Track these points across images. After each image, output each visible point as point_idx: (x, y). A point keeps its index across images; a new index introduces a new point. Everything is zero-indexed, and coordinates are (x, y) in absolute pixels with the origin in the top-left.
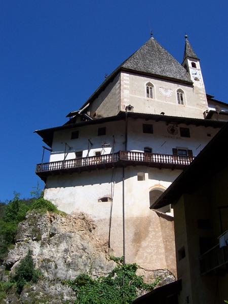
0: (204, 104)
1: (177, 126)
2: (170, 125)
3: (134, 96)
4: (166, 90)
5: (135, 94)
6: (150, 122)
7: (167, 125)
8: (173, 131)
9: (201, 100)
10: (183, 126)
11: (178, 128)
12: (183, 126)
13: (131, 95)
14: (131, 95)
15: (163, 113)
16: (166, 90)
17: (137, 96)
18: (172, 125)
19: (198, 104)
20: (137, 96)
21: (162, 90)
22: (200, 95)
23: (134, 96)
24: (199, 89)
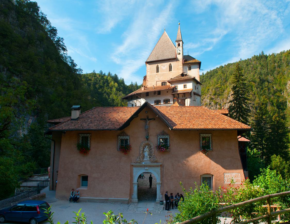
4: (164, 66)
5: (152, 73)
13: (150, 74)
14: (150, 74)
17: (152, 74)
19: (178, 69)
20: (152, 74)
21: (162, 67)
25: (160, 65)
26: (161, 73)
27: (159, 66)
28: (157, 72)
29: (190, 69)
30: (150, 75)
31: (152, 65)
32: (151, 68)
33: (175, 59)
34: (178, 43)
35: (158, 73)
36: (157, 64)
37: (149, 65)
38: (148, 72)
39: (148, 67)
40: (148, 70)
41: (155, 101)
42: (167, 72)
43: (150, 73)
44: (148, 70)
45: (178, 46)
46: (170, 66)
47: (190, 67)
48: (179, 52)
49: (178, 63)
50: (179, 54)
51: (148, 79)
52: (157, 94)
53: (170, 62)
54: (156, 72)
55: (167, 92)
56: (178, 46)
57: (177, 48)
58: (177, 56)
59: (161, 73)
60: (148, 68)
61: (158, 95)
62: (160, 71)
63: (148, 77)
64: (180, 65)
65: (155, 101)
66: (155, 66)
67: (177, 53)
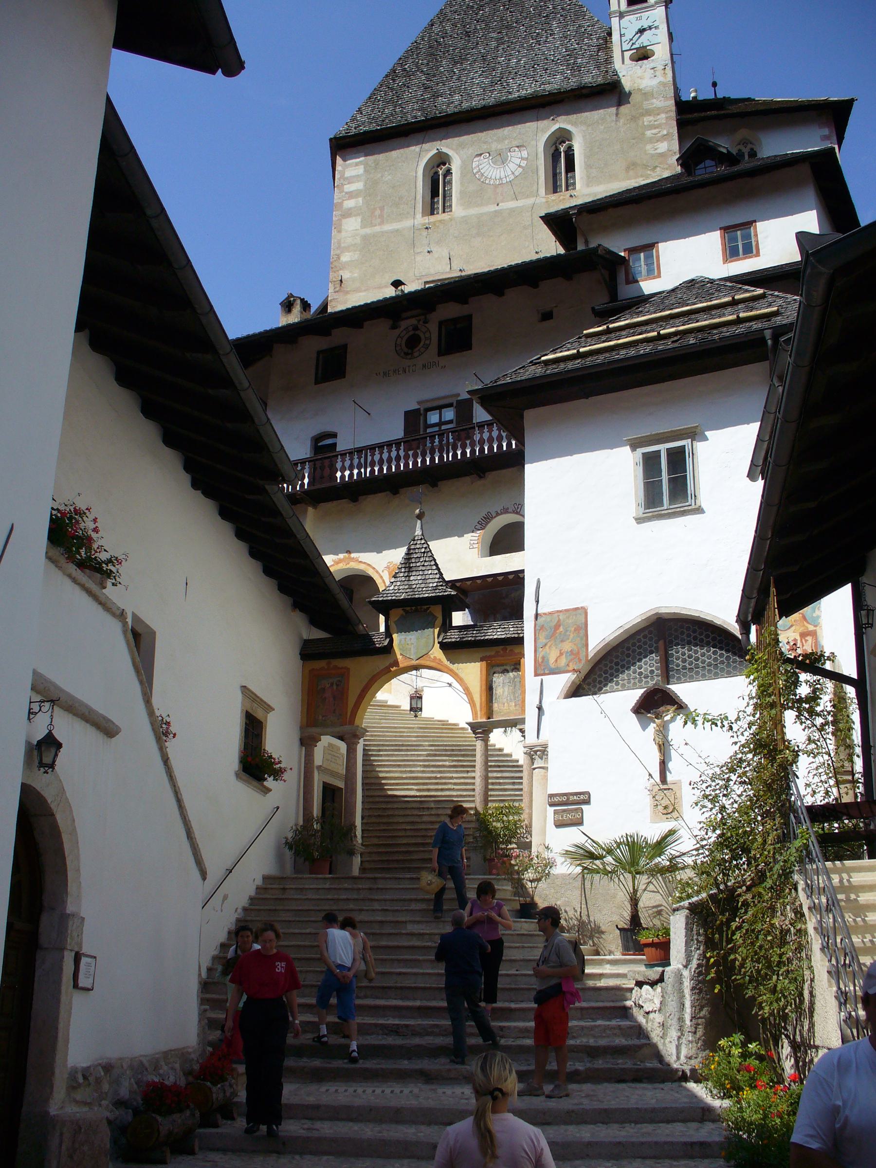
0: (662, 155)
1: (426, 322)
2: (404, 324)
3: (377, 229)
4: (501, 158)
5: (382, 223)
6: (339, 336)
7: (394, 327)
8: (413, 342)
9: (651, 140)
10: (450, 311)
11: (433, 327)
12: (450, 311)
13: (368, 231)
14: (368, 231)
15: (397, 284)
16: (501, 158)
17: (387, 227)
18: (414, 321)
20: (387, 227)
22: (647, 120)
23: (377, 229)
24: (647, 95)
25: (459, 150)
26: (473, 211)
27: (456, 166)
28: (432, 213)
30: (365, 238)
33: (610, 92)
35: (440, 217)
38: (348, 214)
39: (350, 180)
40: (349, 204)
41: (407, 414)
42: (530, 201)
43: (363, 226)
44: (349, 204)
46: (555, 157)
49: (634, 119)
50: (643, 55)
51: (346, 275)
52: (434, 348)
54: (419, 215)
55: (547, 316)
57: (621, 15)
59: (473, 211)
60: (348, 188)
61: (444, 360)
62: (462, 193)
63: (345, 258)
65: (407, 414)
66: (411, 161)
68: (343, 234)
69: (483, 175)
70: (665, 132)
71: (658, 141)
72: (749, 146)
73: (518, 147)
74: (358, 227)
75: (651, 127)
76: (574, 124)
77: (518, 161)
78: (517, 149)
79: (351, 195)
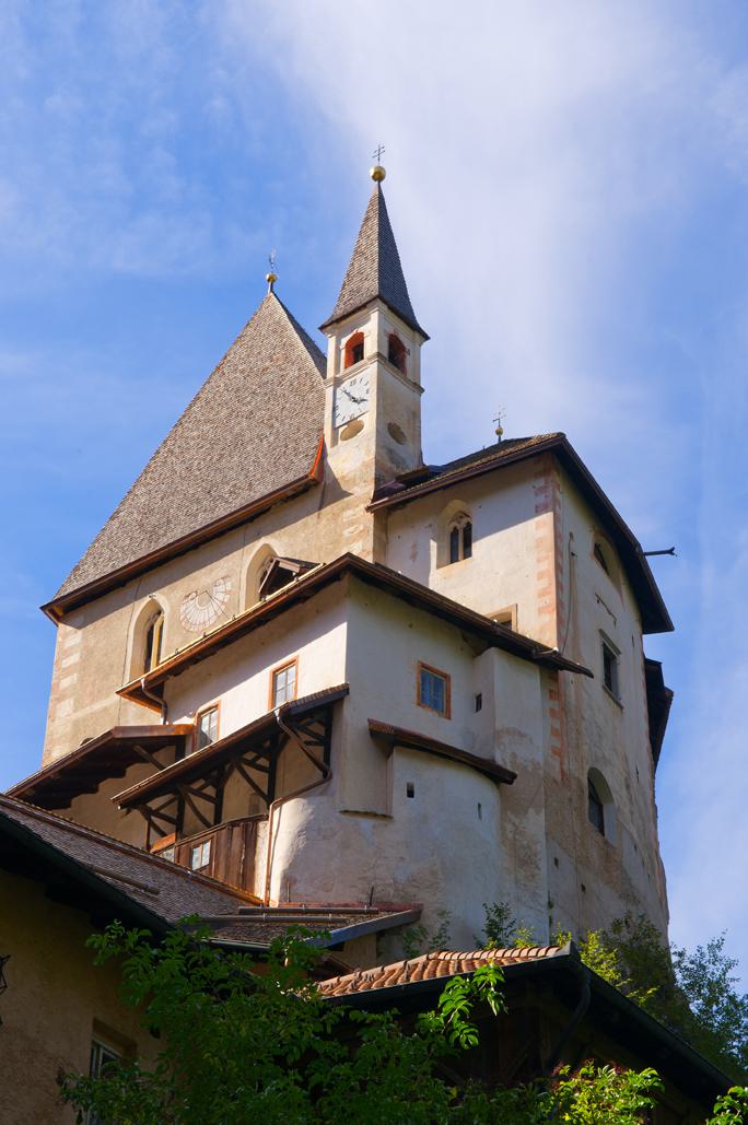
5: (93, 701)
13: (80, 714)
29: (460, 545)
31: (98, 623)
32: (88, 653)
34: (344, 341)
36: (147, 599)
37: (79, 628)
45: (349, 362)
47: (468, 530)
48: (347, 410)
49: (336, 516)
53: (258, 536)
56: (349, 362)
58: (331, 461)
64: (346, 533)
67: (335, 429)
68: (57, 721)
69: (188, 621)
70: (361, 528)
71: (354, 540)
72: (465, 520)
73: (223, 578)
74: (71, 712)
75: (351, 523)
76: (273, 540)
77: (220, 597)
78: (222, 581)
79: (68, 672)
